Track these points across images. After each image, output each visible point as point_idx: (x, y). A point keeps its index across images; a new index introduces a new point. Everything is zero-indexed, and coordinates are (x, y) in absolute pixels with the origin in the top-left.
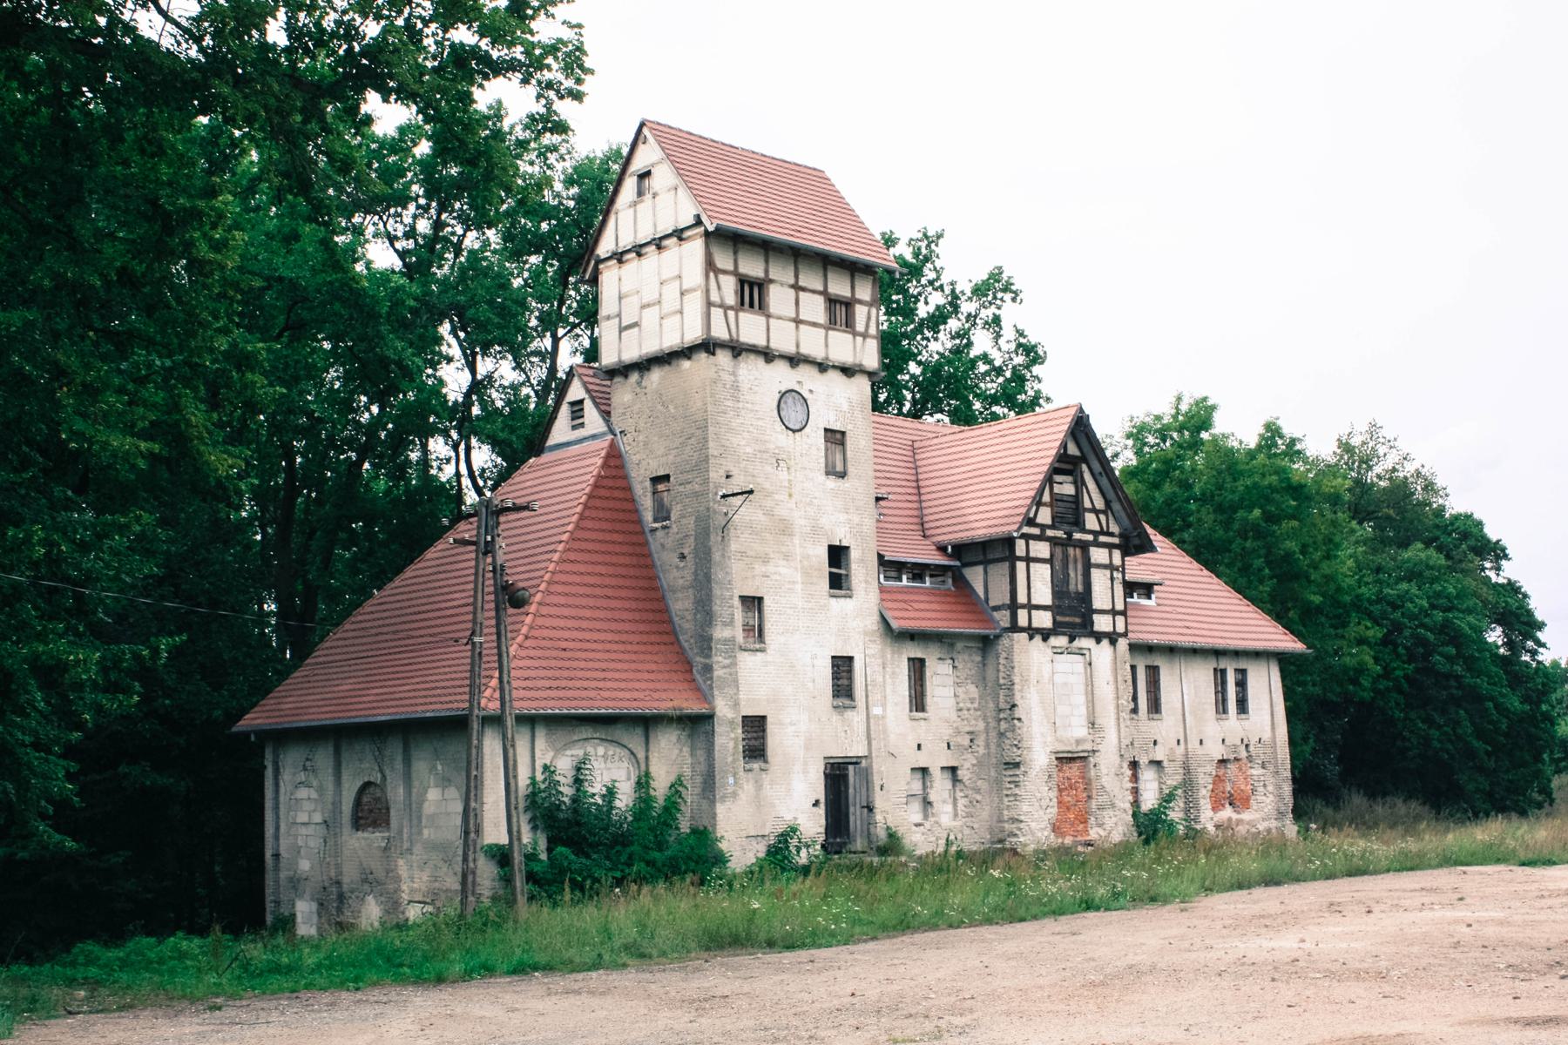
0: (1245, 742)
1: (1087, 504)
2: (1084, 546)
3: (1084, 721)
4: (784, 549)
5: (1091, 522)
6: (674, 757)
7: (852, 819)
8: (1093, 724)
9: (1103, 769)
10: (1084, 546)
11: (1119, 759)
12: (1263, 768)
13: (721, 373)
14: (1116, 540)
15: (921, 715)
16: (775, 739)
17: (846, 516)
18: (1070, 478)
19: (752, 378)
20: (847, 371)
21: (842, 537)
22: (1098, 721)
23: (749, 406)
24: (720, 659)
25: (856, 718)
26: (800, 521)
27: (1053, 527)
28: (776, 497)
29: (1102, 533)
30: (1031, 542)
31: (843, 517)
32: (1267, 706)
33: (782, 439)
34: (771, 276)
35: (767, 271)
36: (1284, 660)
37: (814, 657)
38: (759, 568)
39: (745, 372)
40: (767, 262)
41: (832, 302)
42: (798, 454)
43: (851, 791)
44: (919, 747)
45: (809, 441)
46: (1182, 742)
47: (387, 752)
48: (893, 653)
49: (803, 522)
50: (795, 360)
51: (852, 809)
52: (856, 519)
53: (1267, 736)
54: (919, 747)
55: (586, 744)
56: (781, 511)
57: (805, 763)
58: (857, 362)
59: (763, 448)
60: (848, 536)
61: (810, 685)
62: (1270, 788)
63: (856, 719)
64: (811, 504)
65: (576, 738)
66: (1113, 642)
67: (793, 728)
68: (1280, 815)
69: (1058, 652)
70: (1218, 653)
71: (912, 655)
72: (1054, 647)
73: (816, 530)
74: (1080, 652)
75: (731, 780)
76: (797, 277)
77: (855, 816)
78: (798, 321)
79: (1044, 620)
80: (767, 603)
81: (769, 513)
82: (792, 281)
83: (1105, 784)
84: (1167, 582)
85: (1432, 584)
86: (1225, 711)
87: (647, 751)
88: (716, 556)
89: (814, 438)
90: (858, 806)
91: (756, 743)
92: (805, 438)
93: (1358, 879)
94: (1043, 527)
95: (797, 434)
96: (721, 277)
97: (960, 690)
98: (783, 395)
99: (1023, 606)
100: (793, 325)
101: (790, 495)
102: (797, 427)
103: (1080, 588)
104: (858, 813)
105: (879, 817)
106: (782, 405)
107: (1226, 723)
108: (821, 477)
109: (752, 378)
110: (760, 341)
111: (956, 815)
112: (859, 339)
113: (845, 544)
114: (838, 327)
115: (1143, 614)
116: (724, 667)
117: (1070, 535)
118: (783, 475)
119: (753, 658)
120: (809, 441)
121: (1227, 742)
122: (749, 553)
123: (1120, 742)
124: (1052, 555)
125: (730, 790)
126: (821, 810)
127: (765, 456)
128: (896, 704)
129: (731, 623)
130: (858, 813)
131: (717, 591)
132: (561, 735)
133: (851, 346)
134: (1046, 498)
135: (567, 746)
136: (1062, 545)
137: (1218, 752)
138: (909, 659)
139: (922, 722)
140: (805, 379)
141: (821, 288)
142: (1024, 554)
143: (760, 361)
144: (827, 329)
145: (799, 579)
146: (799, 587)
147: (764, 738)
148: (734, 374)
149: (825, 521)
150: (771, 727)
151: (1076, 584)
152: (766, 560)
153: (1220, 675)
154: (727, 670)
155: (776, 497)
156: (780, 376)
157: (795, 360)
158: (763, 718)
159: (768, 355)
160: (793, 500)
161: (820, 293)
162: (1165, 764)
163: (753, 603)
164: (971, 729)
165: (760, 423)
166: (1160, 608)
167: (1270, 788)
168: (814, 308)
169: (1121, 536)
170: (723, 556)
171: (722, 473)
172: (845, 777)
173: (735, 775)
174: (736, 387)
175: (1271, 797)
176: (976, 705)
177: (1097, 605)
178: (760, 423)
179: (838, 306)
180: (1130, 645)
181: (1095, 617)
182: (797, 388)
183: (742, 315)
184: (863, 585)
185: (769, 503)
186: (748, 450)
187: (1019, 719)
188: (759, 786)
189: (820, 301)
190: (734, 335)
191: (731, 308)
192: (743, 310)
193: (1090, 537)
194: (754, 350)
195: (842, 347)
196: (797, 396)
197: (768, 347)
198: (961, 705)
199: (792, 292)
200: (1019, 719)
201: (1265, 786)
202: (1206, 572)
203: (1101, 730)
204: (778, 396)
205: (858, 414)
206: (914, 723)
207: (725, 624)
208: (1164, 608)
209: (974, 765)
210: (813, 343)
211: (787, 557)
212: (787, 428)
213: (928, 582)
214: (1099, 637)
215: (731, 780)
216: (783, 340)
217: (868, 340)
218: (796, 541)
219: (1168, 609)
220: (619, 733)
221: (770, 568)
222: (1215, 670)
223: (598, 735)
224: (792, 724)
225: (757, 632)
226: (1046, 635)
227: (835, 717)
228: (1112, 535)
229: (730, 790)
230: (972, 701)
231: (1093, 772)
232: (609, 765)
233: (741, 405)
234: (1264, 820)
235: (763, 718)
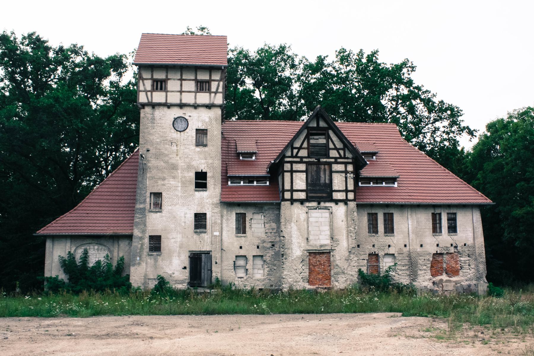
0: (454, 245)
1: (331, 146)
2: (330, 164)
3: (328, 237)
4: (172, 175)
5: (333, 153)
6: (126, 250)
7: (203, 274)
8: (332, 238)
9: (337, 257)
10: (330, 164)
11: (348, 254)
12: (469, 257)
13: (147, 115)
14: (350, 161)
15: (244, 235)
16: (164, 244)
17: (205, 161)
18: (323, 137)
19: (161, 114)
20: (209, 107)
21: (203, 168)
22: (335, 237)
23: (159, 125)
24: (138, 215)
25: (206, 237)
26: (181, 164)
27: (308, 157)
28: (170, 156)
29: (341, 157)
30: (294, 164)
31: (203, 161)
32: (471, 229)
33: (175, 135)
34: (169, 77)
35: (167, 76)
36: (481, 207)
37: (185, 214)
38: (160, 182)
39: (158, 113)
40: (167, 73)
41: (197, 81)
42: (182, 140)
43: (203, 264)
44: (241, 248)
45: (188, 134)
46: (408, 245)
47: (115, 247)
48: (227, 211)
49: (183, 164)
50: (181, 106)
51: (203, 271)
52: (210, 161)
53: (470, 242)
54: (241, 248)
55: (90, 245)
56: (173, 161)
57: (179, 253)
58: (211, 102)
59: (165, 139)
60: (206, 168)
61: (183, 224)
62: (473, 266)
63: (206, 237)
64: (187, 157)
65: (84, 243)
66: (346, 204)
67: (174, 240)
68: (478, 279)
69: (310, 208)
70: (434, 206)
71: (238, 212)
72: (307, 207)
73: (189, 167)
74: (326, 208)
75: (138, 258)
76: (181, 76)
77: (204, 274)
78: (181, 92)
79: (303, 196)
80: (164, 194)
81: (166, 162)
82: (179, 78)
83: (339, 264)
84: (400, 177)
85: (481, 168)
86: (376, 232)
87: (53, 247)
88: (140, 179)
89: (191, 133)
90: (206, 270)
91: (158, 245)
92: (185, 134)
93: (171, 317)
94: (302, 158)
95: (182, 133)
96: (145, 81)
97: (267, 225)
98: (175, 119)
99: (288, 191)
100: (179, 93)
101: (177, 155)
102: (182, 130)
103: (327, 181)
104: (206, 272)
105: (214, 274)
106: (175, 123)
107: (441, 237)
108: (193, 147)
109: (161, 114)
110: (163, 101)
111: (264, 275)
112: (213, 95)
113: (204, 171)
114: (204, 91)
115: (394, 191)
116: (139, 218)
117: (319, 160)
118: (174, 148)
119: (156, 215)
120: (188, 134)
121: (440, 245)
122: (156, 177)
123: (348, 246)
124: (307, 169)
125: (137, 262)
126: (188, 271)
127: (165, 142)
128: (229, 231)
129: (144, 202)
130: (206, 272)
131: (138, 191)
132: (79, 242)
133: (208, 97)
134: (305, 145)
135: (82, 245)
136: (316, 164)
137: (433, 250)
138: (236, 214)
139: (243, 238)
140: (188, 113)
141: (194, 78)
142: (294, 169)
143: (166, 109)
144: (196, 92)
145: (180, 185)
146: (179, 188)
147: (160, 244)
148: (153, 114)
149: (194, 163)
150: (163, 240)
151: (324, 178)
152: (164, 179)
153: (434, 215)
154: (141, 219)
155: (170, 156)
156: (176, 112)
157: (181, 106)
158: (160, 237)
159: (168, 106)
160: (178, 157)
161: (193, 80)
162: (396, 255)
163: (158, 195)
164: (273, 240)
165: (164, 130)
166: (399, 188)
167: (473, 266)
168: (190, 86)
169: (352, 158)
170: (143, 179)
171: (145, 149)
172: (200, 259)
173: (140, 257)
174: (153, 119)
175: (473, 270)
176: (275, 231)
177: (335, 187)
178: (164, 130)
179: (204, 84)
180: (357, 204)
181: (334, 193)
182: (183, 116)
183: (154, 93)
184: (213, 186)
185: (166, 159)
186: (158, 140)
187: (284, 237)
188: (156, 261)
189: (193, 83)
190: (150, 100)
191: (149, 91)
192: (155, 91)
193: (333, 160)
194: (160, 105)
195: (203, 98)
196: (182, 119)
197: (181, 103)
198: (267, 231)
199: (179, 82)
200: (284, 237)
201: (469, 265)
202: (447, 171)
203: (337, 241)
204: (173, 119)
205: (214, 122)
206: (238, 238)
207: (141, 203)
208: (401, 188)
209: (272, 255)
210: (188, 98)
211: (174, 178)
212: (177, 131)
213: (255, 183)
214: (337, 202)
215: (138, 258)
216: (174, 98)
217: (218, 94)
218: (179, 171)
219: (404, 188)
220: (102, 241)
221: (166, 182)
222: (433, 214)
223: (94, 242)
224: (173, 238)
225: (158, 206)
226: (302, 202)
227: (195, 236)
228: (348, 158)
229: (137, 262)
230: (273, 229)
231: (332, 259)
232: (99, 252)
233: (155, 125)
234: (466, 280)
235: (160, 237)
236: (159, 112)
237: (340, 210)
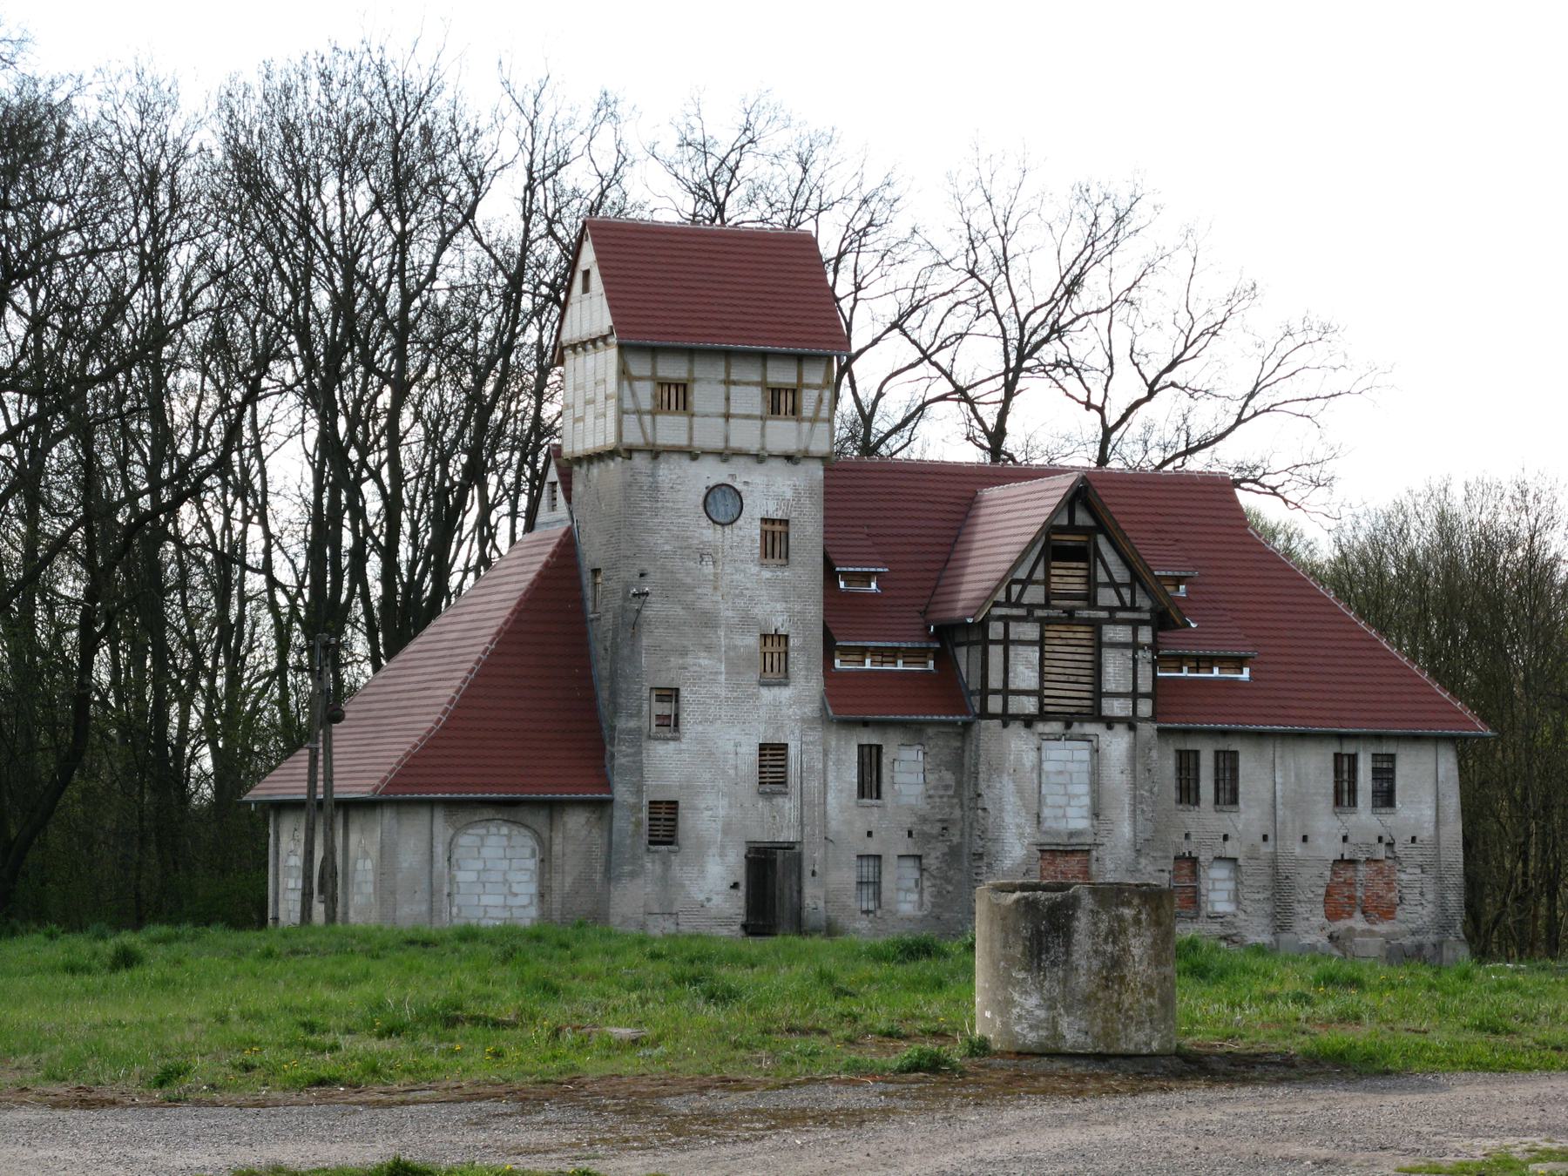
3: (1085, 812)
4: (706, 641)
10: (1096, 626)
14: (1147, 616)
15: (879, 802)
17: (784, 605)
19: (674, 477)
21: (779, 623)
25: (788, 806)
26: (726, 612)
28: (699, 591)
29: (1123, 608)
30: (1012, 625)
31: (780, 606)
33: (709, 534)
38: (675, 661)
39: (666, 472)
44: (870, 834)
48: (839, 740)
49: (730, 613)
52: (798, 608)
54: (870, 834)
56: (706, 605)
57: (723, 847)
61: (732, 772)
63: (787, 806)
64: (742, 594)
69: (1045, 737)
71: (865, 742)
73: (746, 621)
74: (1084, 738)
76: (728, 373)
78: (727, 416)
79: (1030, 705)
80: (684, 693)
81: (688, 607)
89: (749, 530)
92: (736, 531)
94: (1031, 607)
96: (637, 384)
97: (930, 777)
98: (710, 491)
99: (996, 692)
100: (721, 421)
101: (715, 588)
102: (729, 519)
106: (710, 499)
109: (674, 477)
110: (683, 441)
111: (921, 904)
116: (627, 756)
118: (708, 569)
120: (741, 533)
122: (664, 647)
123: (1135, 835)
127: (686, 552)
128: (841, 791)
129: (639, 714)
143: (685, 462)
146: (722, 678)
148: (653, 475)
149: (758, 611)
150: (682, 812)
152: (684, 652)
155: (699, 591)
156: (711, 472)
159: (693, 455)
163: (670, 695)
168: (749, 399)
169: (1152, 611)
171: (636, 571)
174: (655, 488)
183: (659, 418)
185: (690, 597)
186: (667, 547)
187: (984, 809)
188: (666, 865)
193: (1104, 614)
198: (931, 792)
199: (722, 388)
204: (704, 491)
206: (863, 810)
207: (631, 716)
210: (745, 435)
212: (715, 522)
214: (1110, 723)
216: (708, 434)
218: (722, 633)
221: (689, 660)
224: (707, 809)
225: (671, 724)
226: (1028, 721)
228: (1139, 610)
230: (947, 787)
231: (1094, 867)
233: (660, 505)
235: (676, 803)
236: (668, 471)
237: (1117, 744)
